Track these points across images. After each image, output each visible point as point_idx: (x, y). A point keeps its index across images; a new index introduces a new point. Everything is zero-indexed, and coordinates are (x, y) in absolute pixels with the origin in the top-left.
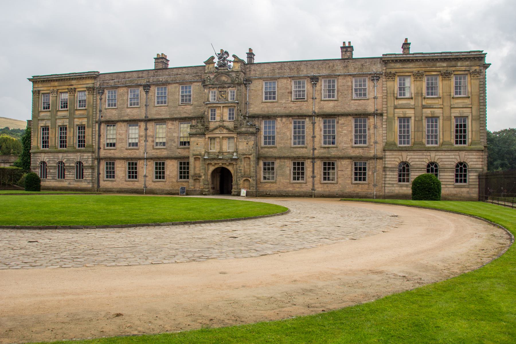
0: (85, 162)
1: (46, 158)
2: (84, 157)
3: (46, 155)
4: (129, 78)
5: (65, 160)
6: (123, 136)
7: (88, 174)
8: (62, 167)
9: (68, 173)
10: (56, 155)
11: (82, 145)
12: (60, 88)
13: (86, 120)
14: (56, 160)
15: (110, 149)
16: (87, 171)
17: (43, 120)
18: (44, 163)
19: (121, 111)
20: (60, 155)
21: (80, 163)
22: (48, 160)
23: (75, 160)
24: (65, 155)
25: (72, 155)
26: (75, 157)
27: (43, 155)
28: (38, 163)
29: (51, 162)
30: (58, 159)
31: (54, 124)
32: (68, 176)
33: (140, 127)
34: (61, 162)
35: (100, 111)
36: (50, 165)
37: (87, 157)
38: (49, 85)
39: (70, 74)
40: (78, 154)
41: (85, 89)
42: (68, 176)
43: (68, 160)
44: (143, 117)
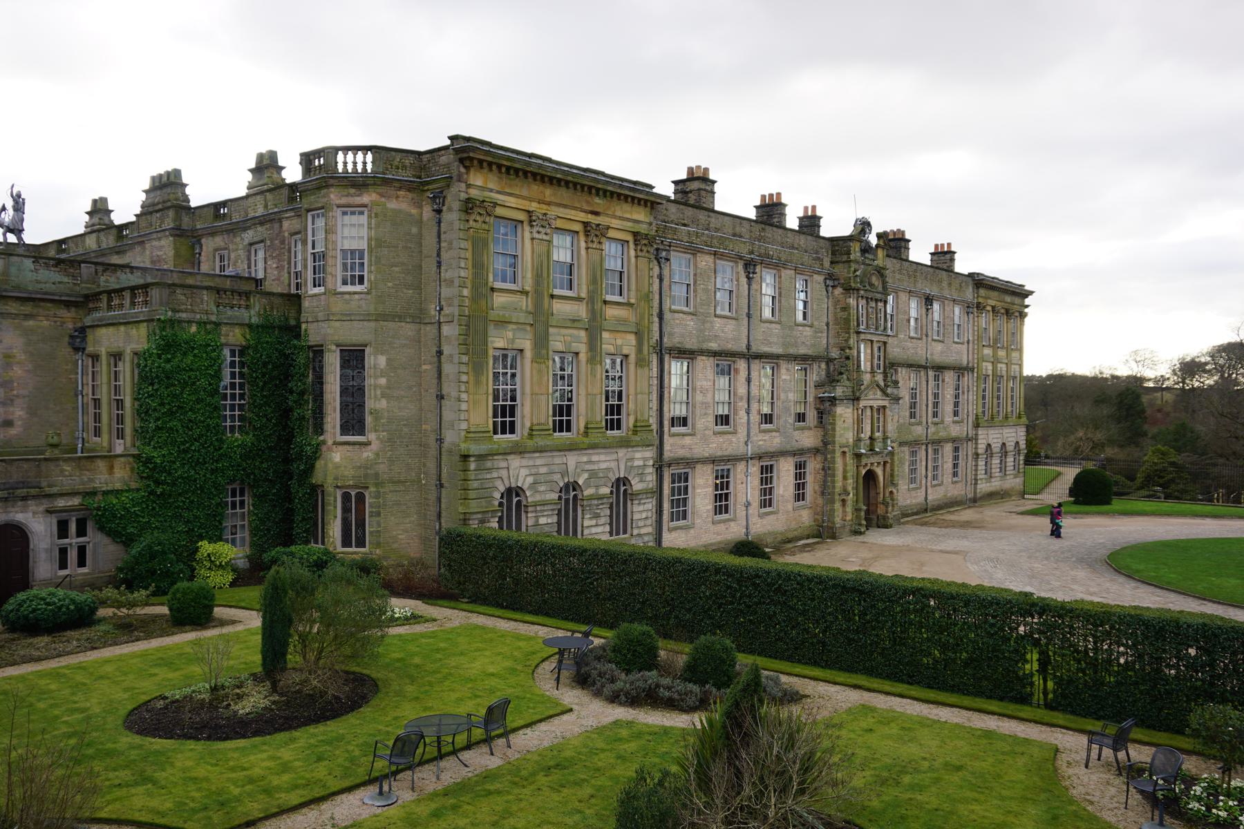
0: (637, 479)
1: (524, 472)
2: (636, 463)
3: (525, 462)
4: (717, 230)
5: (586, 475)
6: (709, 398)
7: (644, 515)
8: (567, 501)
9: (593, 522)
10: (557, 461)
11: (504, 416)
12: (562, 212)
13: (632, 339)
14: (557, 477)
15: (684, 435)
16: (641, 508)
17: (502, 323)
18: (512, 492)
19: (704, 322)
20: (572, 460)
21: (621, 482)
22: (530, 480)
23: (611, 475)
24: (585, 459)
25: (603, 457)
26: (613, 465)
27: (515, 462)
28: (498, 495)
29: (542, 488)
30: (565, 473)
31: (541, 342)
32: (594, 530)
33: (736, 371)
34: (575, 486)
35: (661, 316)
36: (538, 498)
37: (641, 463)
38: (525, 192)
39: (635, 183)
40: (622, 452)
41: (630, 238)
42: (594, 530)
43: (593, 474)
44: (742, 347)
